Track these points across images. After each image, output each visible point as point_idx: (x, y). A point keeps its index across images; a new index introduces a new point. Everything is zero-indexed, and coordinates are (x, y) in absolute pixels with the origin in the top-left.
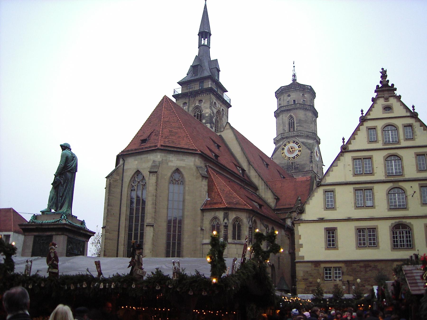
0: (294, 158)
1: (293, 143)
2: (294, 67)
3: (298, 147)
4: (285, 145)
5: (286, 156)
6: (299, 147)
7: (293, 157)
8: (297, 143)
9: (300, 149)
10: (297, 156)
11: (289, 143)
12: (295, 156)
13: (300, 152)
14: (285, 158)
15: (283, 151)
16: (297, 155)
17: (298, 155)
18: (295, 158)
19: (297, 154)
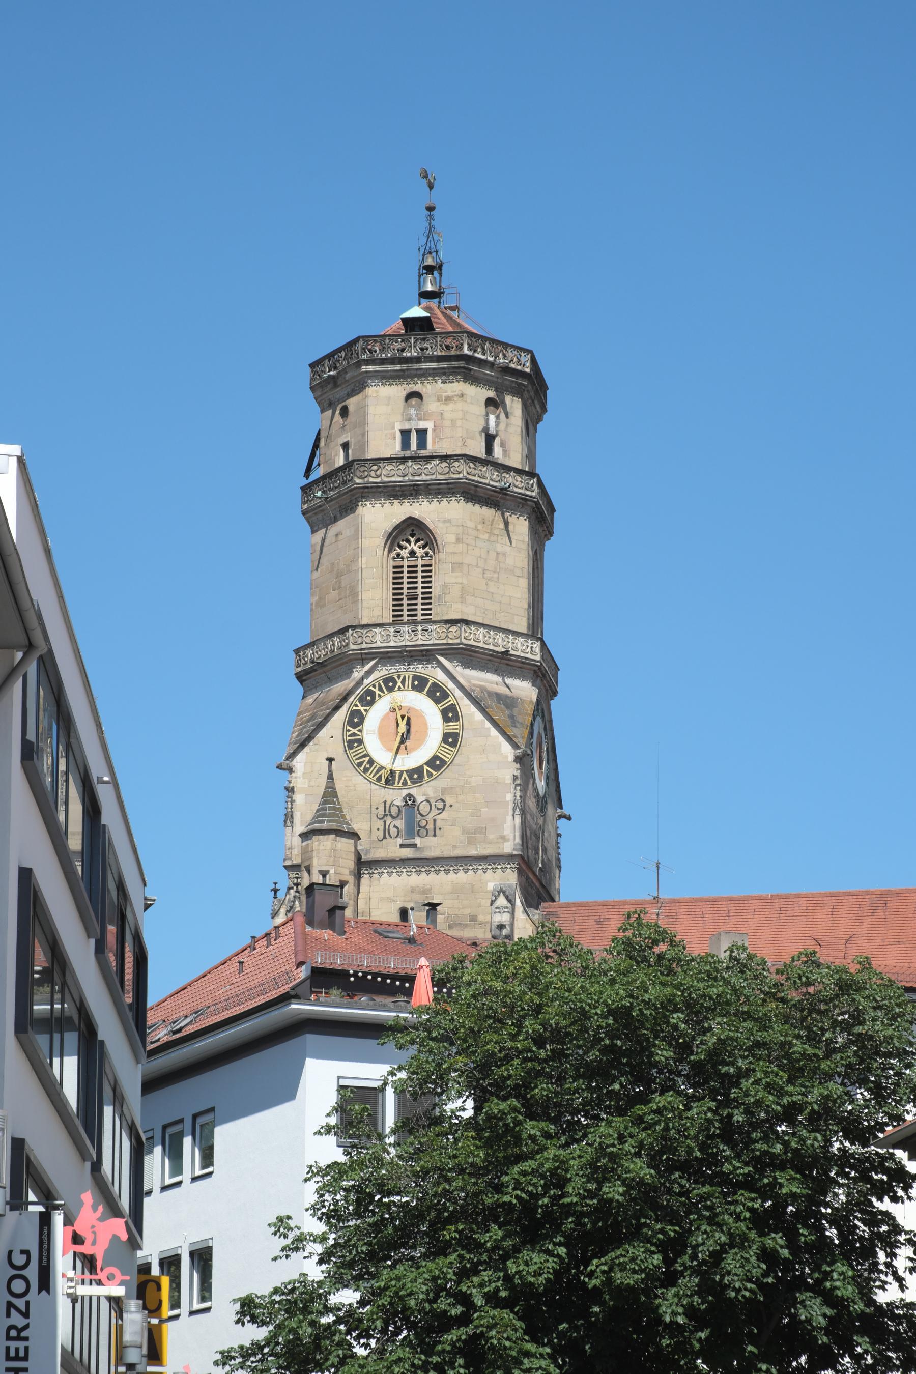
0: (416, 775)
1: (414, 688)
2: (430, 209)
3: (444, 713)
4: (369, 699)
5: (371, 762)
6: (450, 714)
7: (410, 773)
8: (437, 694)
9: (453, 727)
10: (437, 768)
11: (389, 684)
12: (422, 767)
13: (453, 745)
14: (366, 770)
15: (353, 731)
16: (436, 763)
17: (443, 762)
18: (421, 777)
19: (435, 758)
